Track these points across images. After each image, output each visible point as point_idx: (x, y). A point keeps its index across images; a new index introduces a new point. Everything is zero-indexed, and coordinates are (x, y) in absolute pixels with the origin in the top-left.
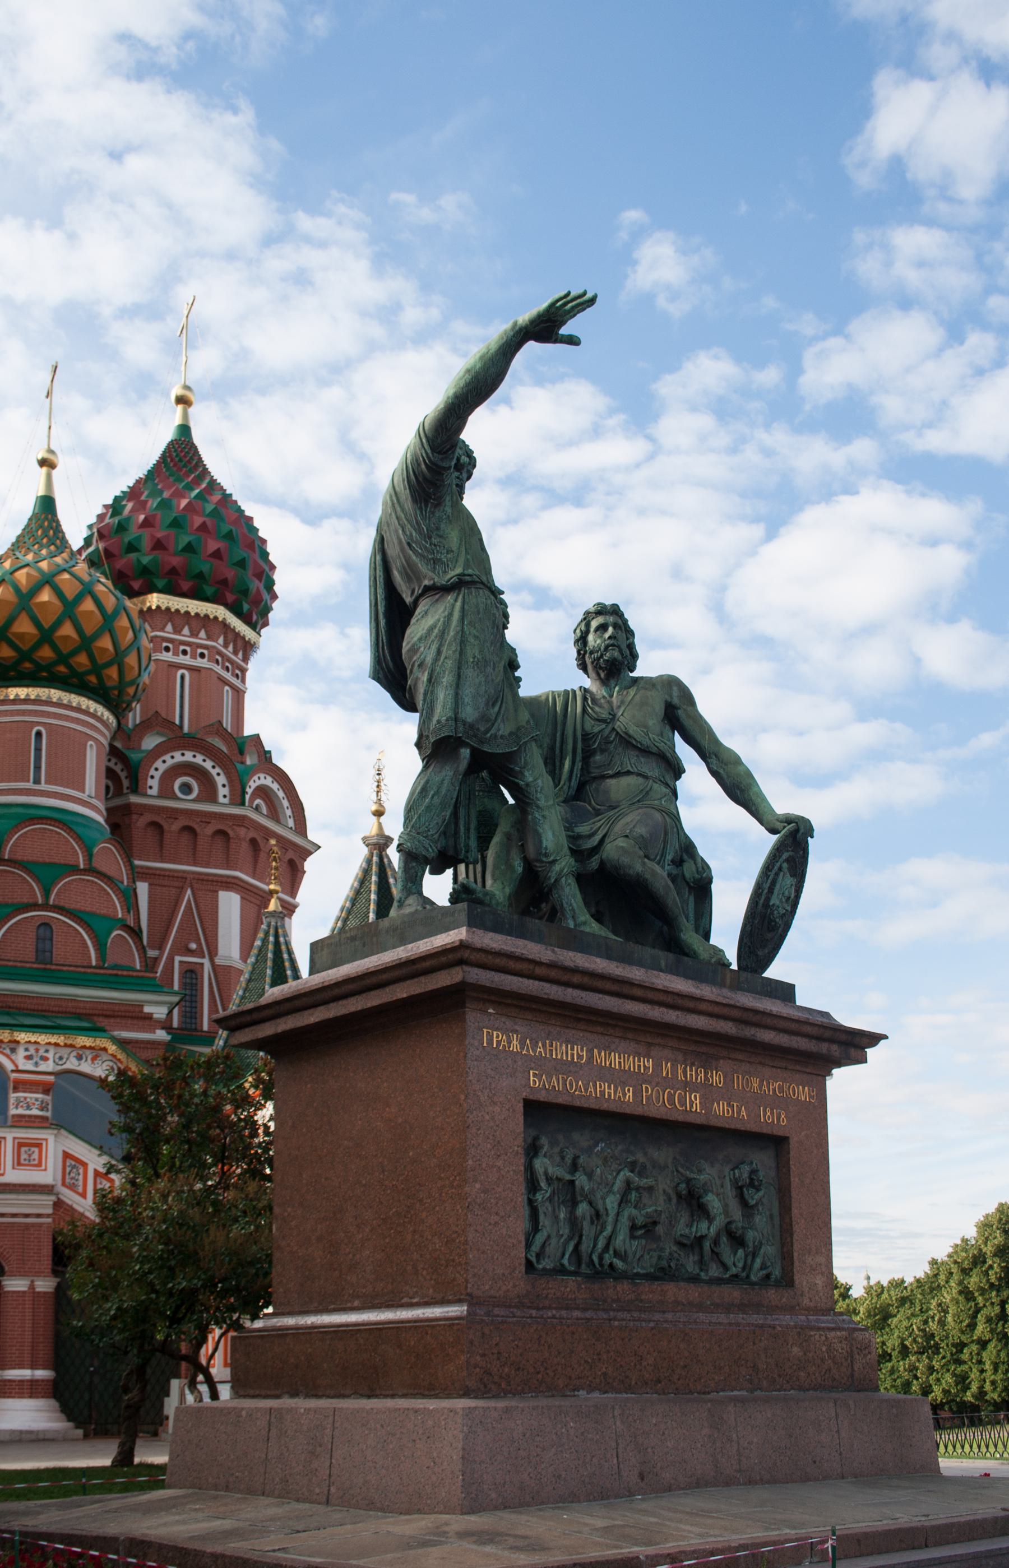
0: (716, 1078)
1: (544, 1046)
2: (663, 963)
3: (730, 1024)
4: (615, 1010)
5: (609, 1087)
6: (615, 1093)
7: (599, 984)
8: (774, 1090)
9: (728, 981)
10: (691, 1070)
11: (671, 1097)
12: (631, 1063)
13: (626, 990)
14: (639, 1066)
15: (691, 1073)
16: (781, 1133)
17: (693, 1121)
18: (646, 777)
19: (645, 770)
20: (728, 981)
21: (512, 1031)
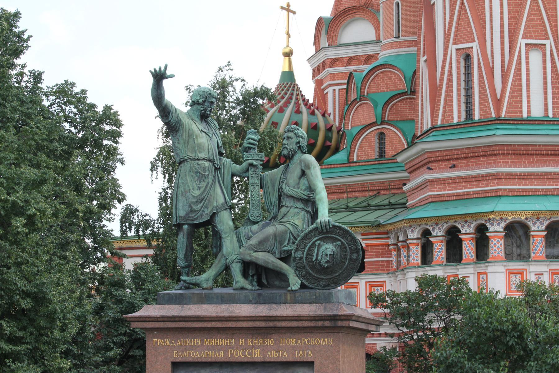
0: (271, 342)
1: (181, 342)
2: (251, 298)
3: (261, 322)
4: (200, 326)
5: (212, 353)
6: (214, 354)
7: (186, 319)
8: (305, 343)
9: (289, 298)
10: (256, 340)
11: (244, 353)
12: (223, 342)
13: (201, 319)
14: (227, 343)
15: (256, 341)
16: (310, 360)
17: (256, 361)
18: (287, 207)
19: (288, 204)
20: (289, 298)
21: (166, 338)
